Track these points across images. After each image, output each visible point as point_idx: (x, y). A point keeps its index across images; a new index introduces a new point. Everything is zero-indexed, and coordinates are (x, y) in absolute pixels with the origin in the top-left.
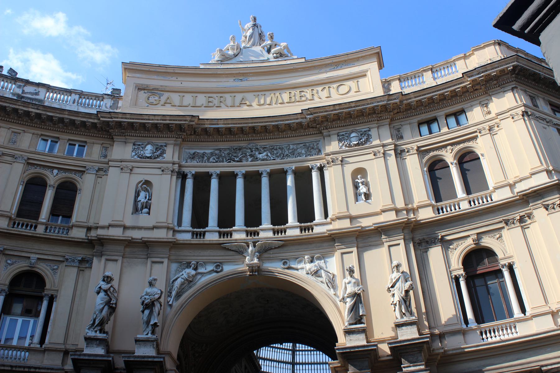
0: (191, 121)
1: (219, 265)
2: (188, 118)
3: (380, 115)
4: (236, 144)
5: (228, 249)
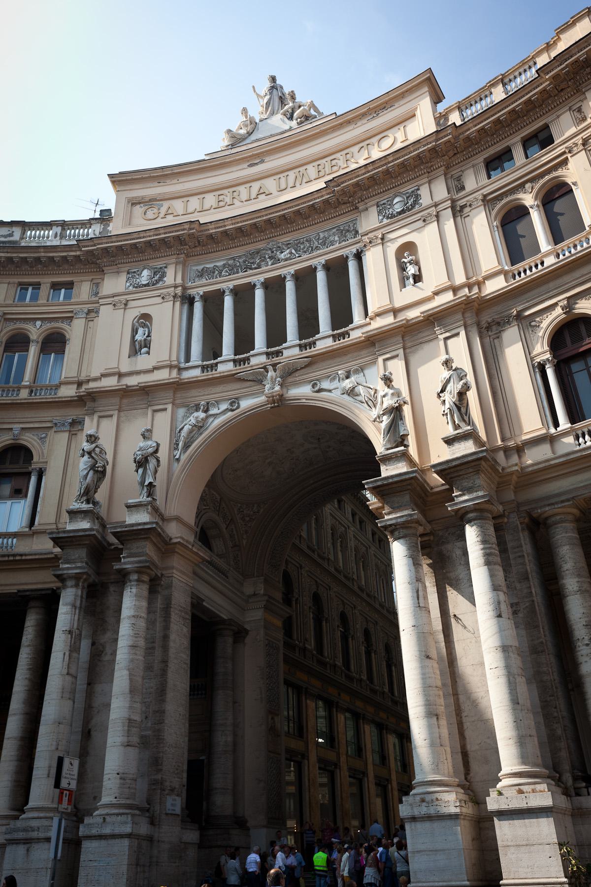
0: (190, 229)
1: (234, 402)
2: (187, 226)
3: (430, 164)
4: (252, 248)
5: (244, 380)
